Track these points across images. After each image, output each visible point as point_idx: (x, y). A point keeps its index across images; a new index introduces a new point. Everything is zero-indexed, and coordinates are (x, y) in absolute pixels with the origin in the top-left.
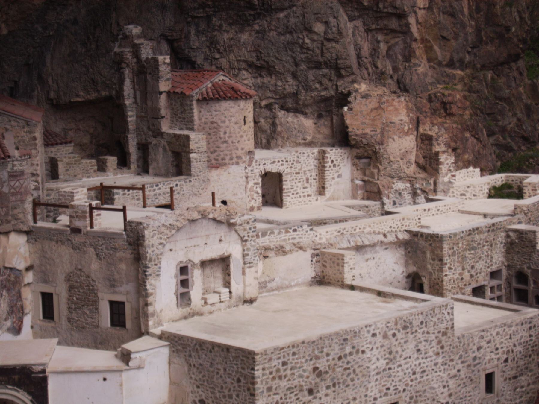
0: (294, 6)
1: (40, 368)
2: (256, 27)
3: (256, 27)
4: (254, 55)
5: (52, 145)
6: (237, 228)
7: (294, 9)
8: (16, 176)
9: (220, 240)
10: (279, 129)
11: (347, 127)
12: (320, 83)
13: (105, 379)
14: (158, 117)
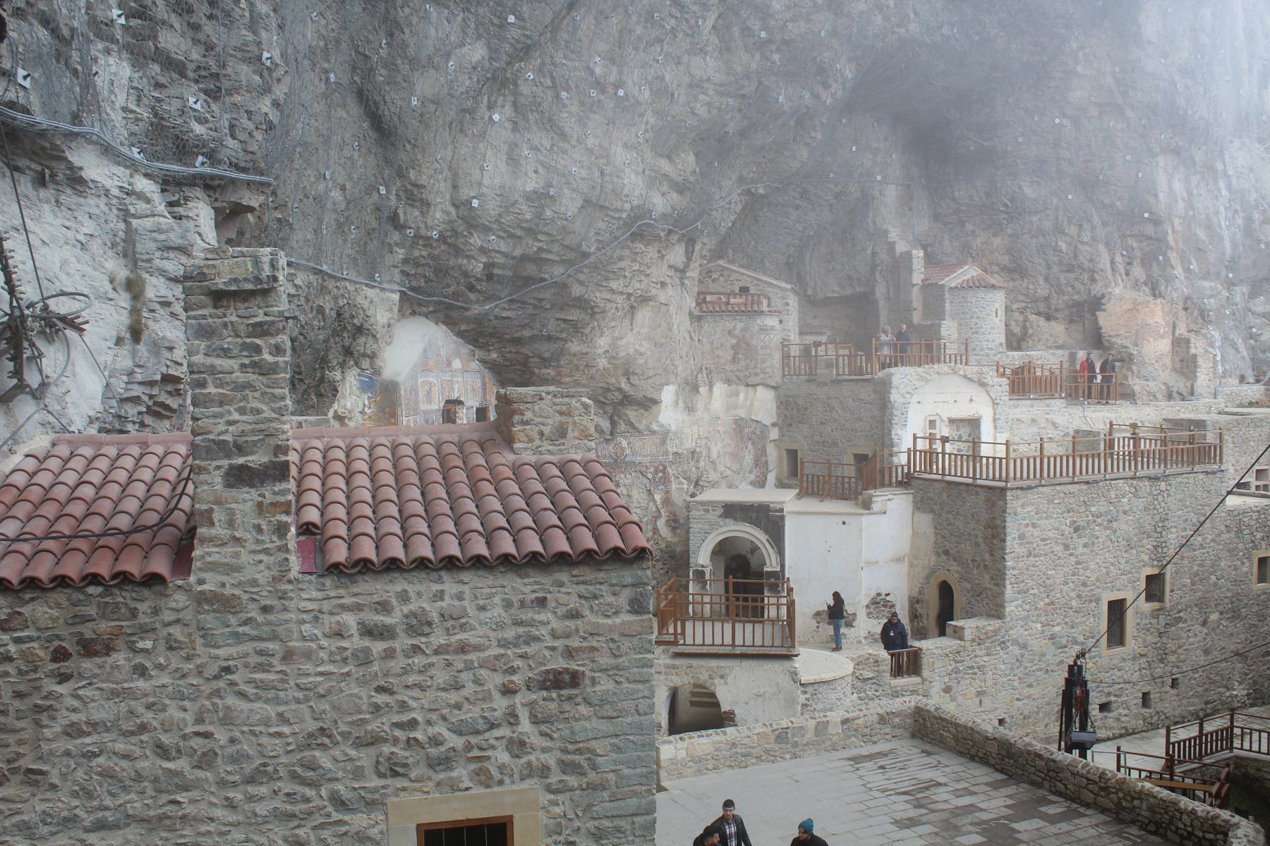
0: (1047, 209)
1: (778, 506)
3: (1009, 231)
4: (1006, 258)
5: (807, 334)
8: (766, 330)
9: (971, 400)
10: (1030, 331)
11: (1100, 328)
12: (1073, 287)
13: (844, 523)
14: (910, 310)
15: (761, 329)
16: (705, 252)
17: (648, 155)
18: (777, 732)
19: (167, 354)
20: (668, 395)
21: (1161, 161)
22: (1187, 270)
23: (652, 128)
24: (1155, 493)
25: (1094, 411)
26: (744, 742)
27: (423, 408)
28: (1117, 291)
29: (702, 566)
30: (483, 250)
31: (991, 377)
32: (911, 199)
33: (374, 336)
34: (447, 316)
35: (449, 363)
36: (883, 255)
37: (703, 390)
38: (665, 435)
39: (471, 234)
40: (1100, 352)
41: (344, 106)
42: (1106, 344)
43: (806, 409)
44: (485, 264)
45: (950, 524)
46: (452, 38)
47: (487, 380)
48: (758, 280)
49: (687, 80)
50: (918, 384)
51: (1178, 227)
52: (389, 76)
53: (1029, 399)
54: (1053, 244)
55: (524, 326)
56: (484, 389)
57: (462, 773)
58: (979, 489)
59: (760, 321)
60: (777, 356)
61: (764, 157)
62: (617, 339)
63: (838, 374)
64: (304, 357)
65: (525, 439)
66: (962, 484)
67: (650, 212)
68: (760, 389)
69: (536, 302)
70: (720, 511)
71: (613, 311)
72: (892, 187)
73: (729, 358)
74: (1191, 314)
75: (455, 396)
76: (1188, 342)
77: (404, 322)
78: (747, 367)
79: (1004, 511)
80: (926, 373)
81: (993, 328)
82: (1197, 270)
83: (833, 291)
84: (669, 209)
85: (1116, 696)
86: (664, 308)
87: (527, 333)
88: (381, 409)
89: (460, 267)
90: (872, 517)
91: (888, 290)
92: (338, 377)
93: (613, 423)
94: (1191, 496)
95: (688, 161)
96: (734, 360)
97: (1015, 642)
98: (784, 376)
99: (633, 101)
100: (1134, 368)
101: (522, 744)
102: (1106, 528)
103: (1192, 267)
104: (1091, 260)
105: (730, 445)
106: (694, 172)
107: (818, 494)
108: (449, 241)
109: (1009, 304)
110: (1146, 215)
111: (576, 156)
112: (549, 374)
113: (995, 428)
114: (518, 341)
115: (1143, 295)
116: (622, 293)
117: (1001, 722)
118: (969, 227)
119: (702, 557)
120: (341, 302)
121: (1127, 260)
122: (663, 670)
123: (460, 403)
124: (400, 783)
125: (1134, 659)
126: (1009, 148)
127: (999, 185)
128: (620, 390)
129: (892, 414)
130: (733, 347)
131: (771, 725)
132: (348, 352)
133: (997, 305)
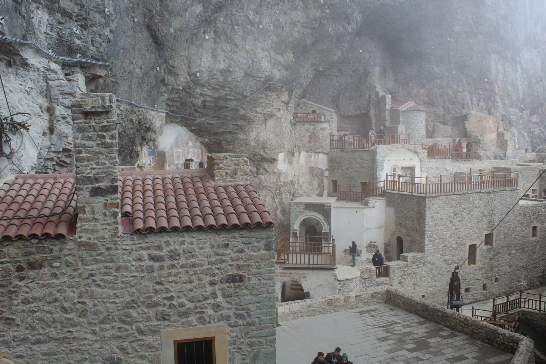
1: (329, 205)
2: (428, 87)
3: (428, 87)
4: (426, 98)
5: (341, 131)
6: (418, 154)
7: (444, 78)
8: (323, 129)
9: (411, 159)
10: (436, 130)
11: (466, 128)
12: (455, 111)
13: (356, 212)
14: (385, 120)
15: (321, 129)
16: (297, 96)
17: (273, 53)
18: (328, 301)
19: (65, 139)
20: (281, 157)
21: (493, 57)
22: (503, 104)
23: (274, 42)
24: (489, 199)
25: (463, 164)
26: (314, 305)
27: (176, 163)
28: (474, 112)
29: (296, 230)
30: (201, 95)
31: (420, 149)
32: (386, 73)
33: (155, 132)
34: (186, 123)
35: (187, 144)
36: (373, 97)
37: (296, 155)
38: (280, 174)
39: (196, 88)
40: (466, 139)
41: (141, 32)
42: (469, 135)
43: (340, 163)
44: (202, 101)
45: (402, 212)
46: (188, 3)
47: (203, 150)
48: (320, 107)
49: (289, 21)
50: (388, 152)
51: (500, 86)
52: (161, 19)
53: (436, 159)
54: (446, 92)
55: (219, 128)
56: (202, 155)
57: (193, 318)
58: (414, 197)
59: (321, 125)
60: (328, 140)
61: (322, 54)
62: (259, 133)
63: (354, 148)
64: (125, 141)
65: (220, 176)
66: (407, 195)
67: (273, 78)
68: (320, 154)
69: (224, 117)
70: (303, 207)
71: (257, 121)
72: (377, 68)
73: (307, 141)
74: (505, 122)
75: (190, 157)
76: (503, 134)
77: (168, 126)
78: (315, 145)
79: (425, 207)
80: (392, 147)
81: (420, 128)
82: (508, 104)
83: (352, 113)
84: (282, 77)
85: (472, 285)
86: (279, 120)
87: (221, 130)
88: (158, 163)
89: (191, 102)
90: (369, 209)
91: (376, 112)
92: (139, 150)
93: (258, 169)
94: (504, 200)
95: (290, 56)
96: (309, 142)
97: (429, 263)
98: (331, 149)
99: (266, 30)
100: (481, 145)
101: (219, 306)
102: (468, 214)
103: (505, 102)
104: (462, 99)
105: (308, 178)
106: (292, 61)
107: (345, 199)
108: (187, 91)
109: (427, 118)
110: (486, 80)
111: (242, 54)
112: (230, 148)
113: (421, 171)
114: (217, 134)
115: (484, 115)
116: (261, 113)
117: (423, 296)
118: (410, 85)
119: (296, 227)
120: (141, 117)
121: (478, 99)
122: (279, 275)
123: (192, 160)
124: (166, 323)
125: (480, 270)
126: (428, 51)
127: (423, 67)
128: (260, 155)
129: (377, 165)
130: (309, 136)
131: (325, 298)
132: (143, 139)
133: (422, 119)
